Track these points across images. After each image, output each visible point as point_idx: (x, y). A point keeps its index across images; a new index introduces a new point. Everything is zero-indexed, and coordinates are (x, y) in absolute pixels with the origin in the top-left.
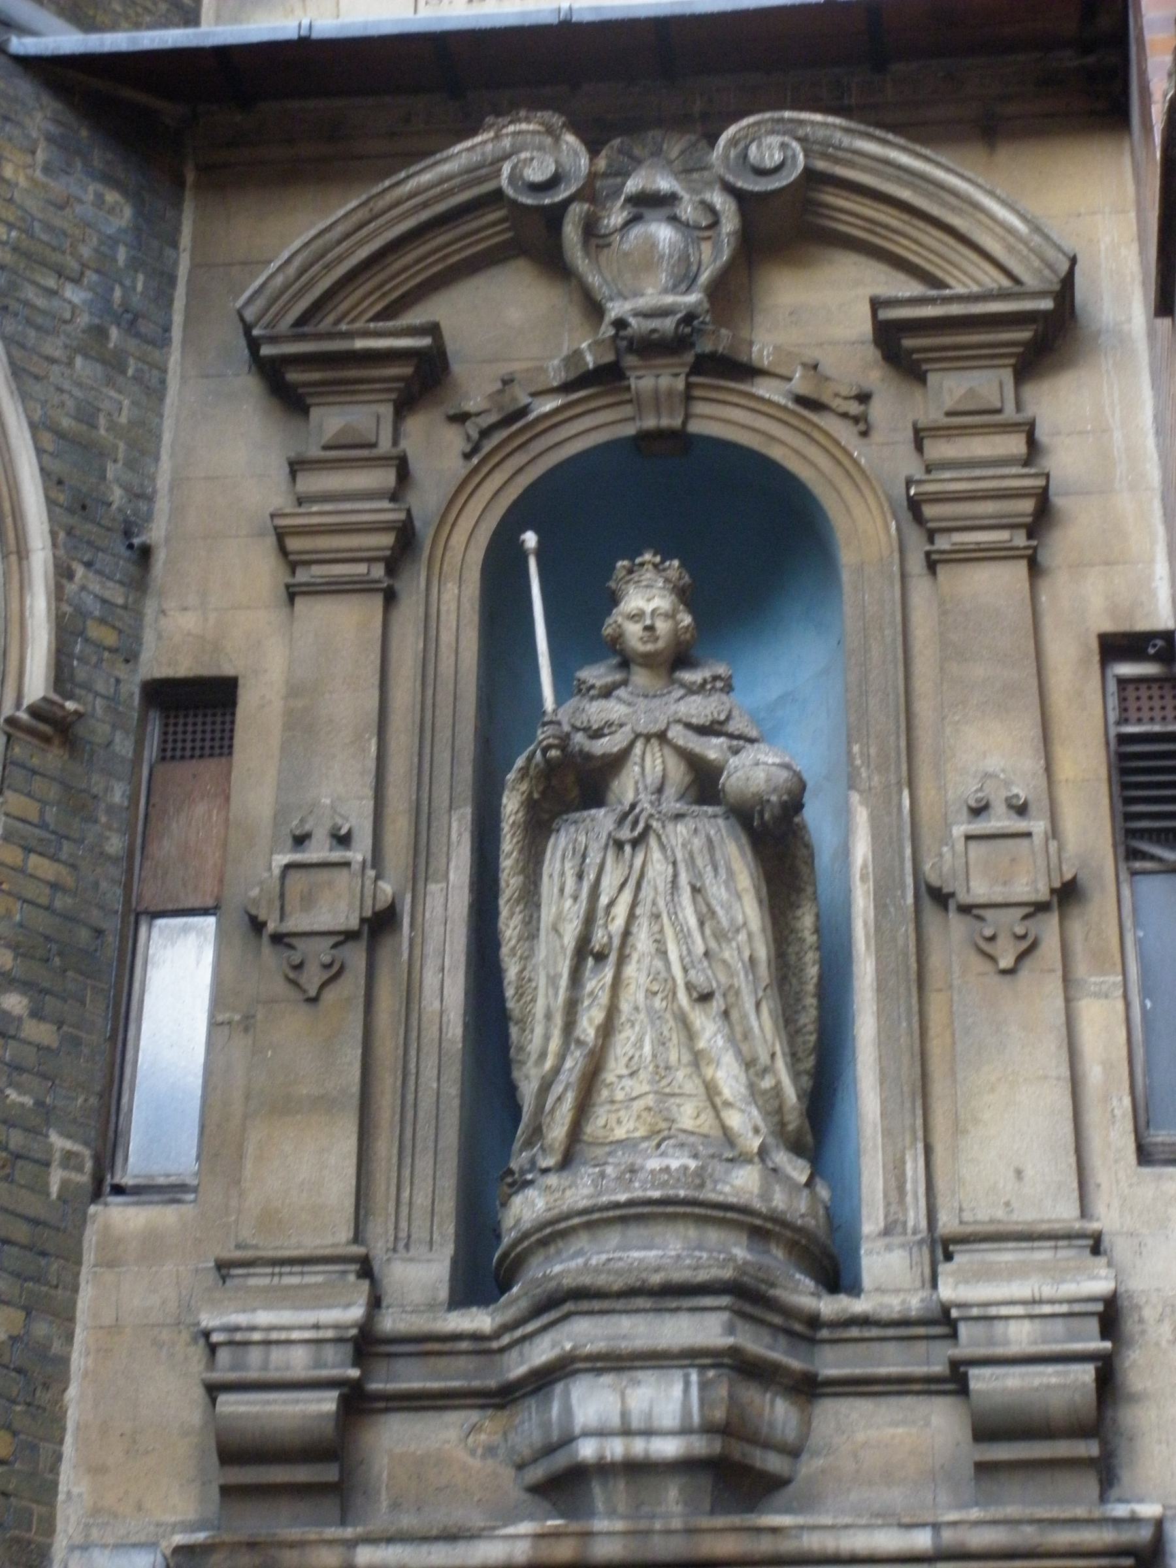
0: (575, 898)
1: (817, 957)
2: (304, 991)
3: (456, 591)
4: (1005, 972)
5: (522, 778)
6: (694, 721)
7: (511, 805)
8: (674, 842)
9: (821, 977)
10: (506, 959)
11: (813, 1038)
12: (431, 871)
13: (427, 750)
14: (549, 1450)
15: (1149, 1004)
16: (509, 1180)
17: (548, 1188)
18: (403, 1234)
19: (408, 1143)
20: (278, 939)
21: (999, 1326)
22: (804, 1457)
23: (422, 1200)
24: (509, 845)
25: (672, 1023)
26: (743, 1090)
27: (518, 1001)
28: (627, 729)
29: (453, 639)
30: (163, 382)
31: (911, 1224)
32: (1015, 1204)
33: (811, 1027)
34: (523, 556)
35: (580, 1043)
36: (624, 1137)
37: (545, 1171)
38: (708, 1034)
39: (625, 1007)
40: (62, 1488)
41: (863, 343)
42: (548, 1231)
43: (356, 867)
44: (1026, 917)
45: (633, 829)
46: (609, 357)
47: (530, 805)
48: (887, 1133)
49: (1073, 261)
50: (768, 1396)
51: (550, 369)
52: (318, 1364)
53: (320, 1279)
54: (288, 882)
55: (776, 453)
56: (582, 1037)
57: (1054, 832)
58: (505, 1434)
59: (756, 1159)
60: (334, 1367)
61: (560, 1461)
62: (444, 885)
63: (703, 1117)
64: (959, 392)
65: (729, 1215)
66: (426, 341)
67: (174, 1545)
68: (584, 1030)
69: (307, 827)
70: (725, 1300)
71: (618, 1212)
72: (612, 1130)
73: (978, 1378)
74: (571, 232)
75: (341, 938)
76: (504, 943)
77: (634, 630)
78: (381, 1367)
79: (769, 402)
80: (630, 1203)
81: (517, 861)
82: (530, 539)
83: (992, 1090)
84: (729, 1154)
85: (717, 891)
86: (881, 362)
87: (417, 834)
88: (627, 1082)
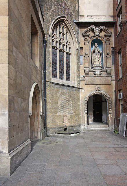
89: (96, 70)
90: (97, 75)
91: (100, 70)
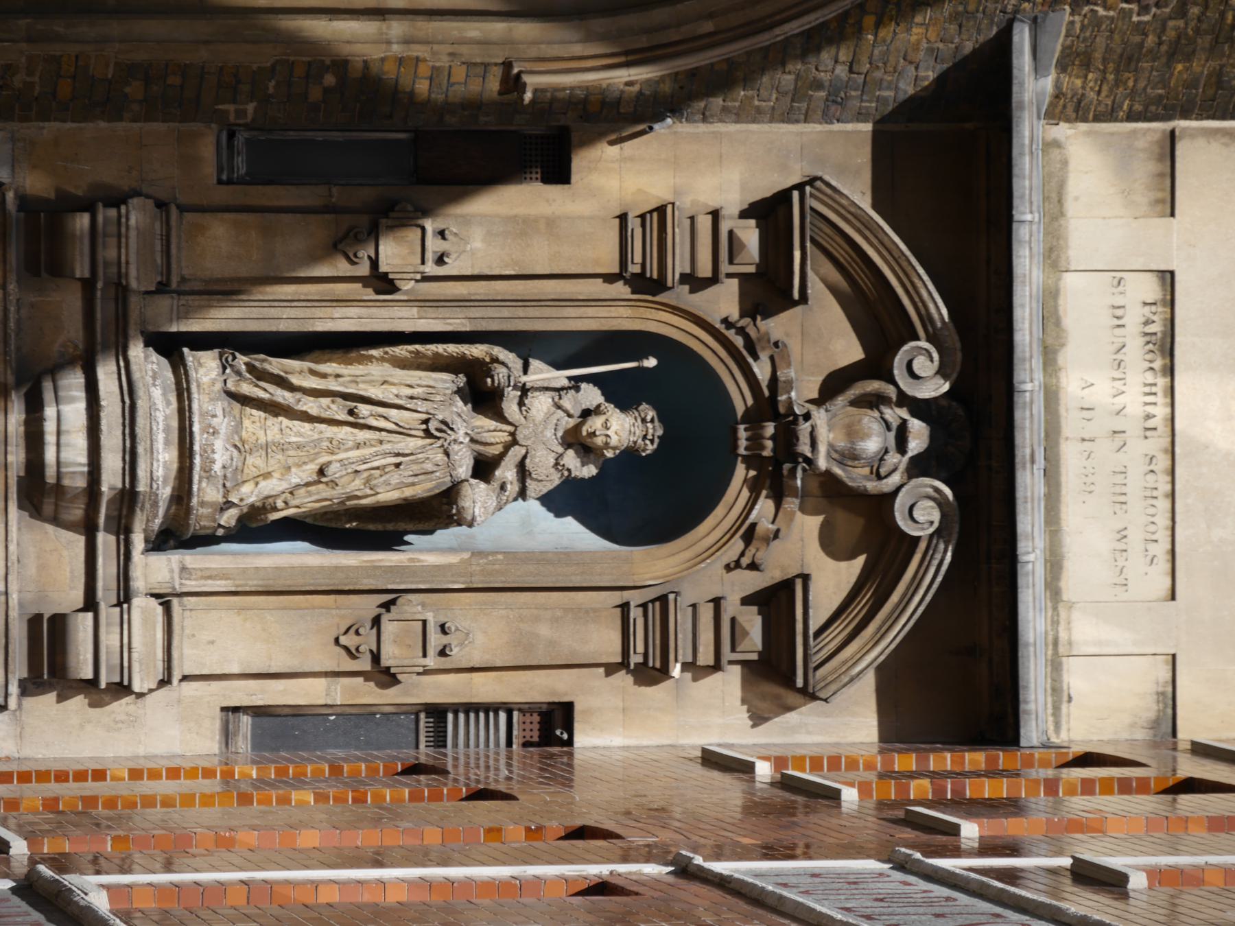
4: (337, 640)
6: (528, 461)
7: (477, 351)
15: (332, 718)
17: (214, 384)
24: (452, 349)
30: (797, 121)
34: (638, 358)
40: (46, 124)
46: (782, 410)
48: (244, 570)
49: (826, 700)
52: (106, 264)
53: (159, 261)
55: (719, 511)
57: (427, 672)
60: (105, 273)
64: (747, 626)
66: (796, 295)
74: (874, 386)
80: (191, 433)
82: (651, 362)
84: (228, 484)
91: (112, 478)
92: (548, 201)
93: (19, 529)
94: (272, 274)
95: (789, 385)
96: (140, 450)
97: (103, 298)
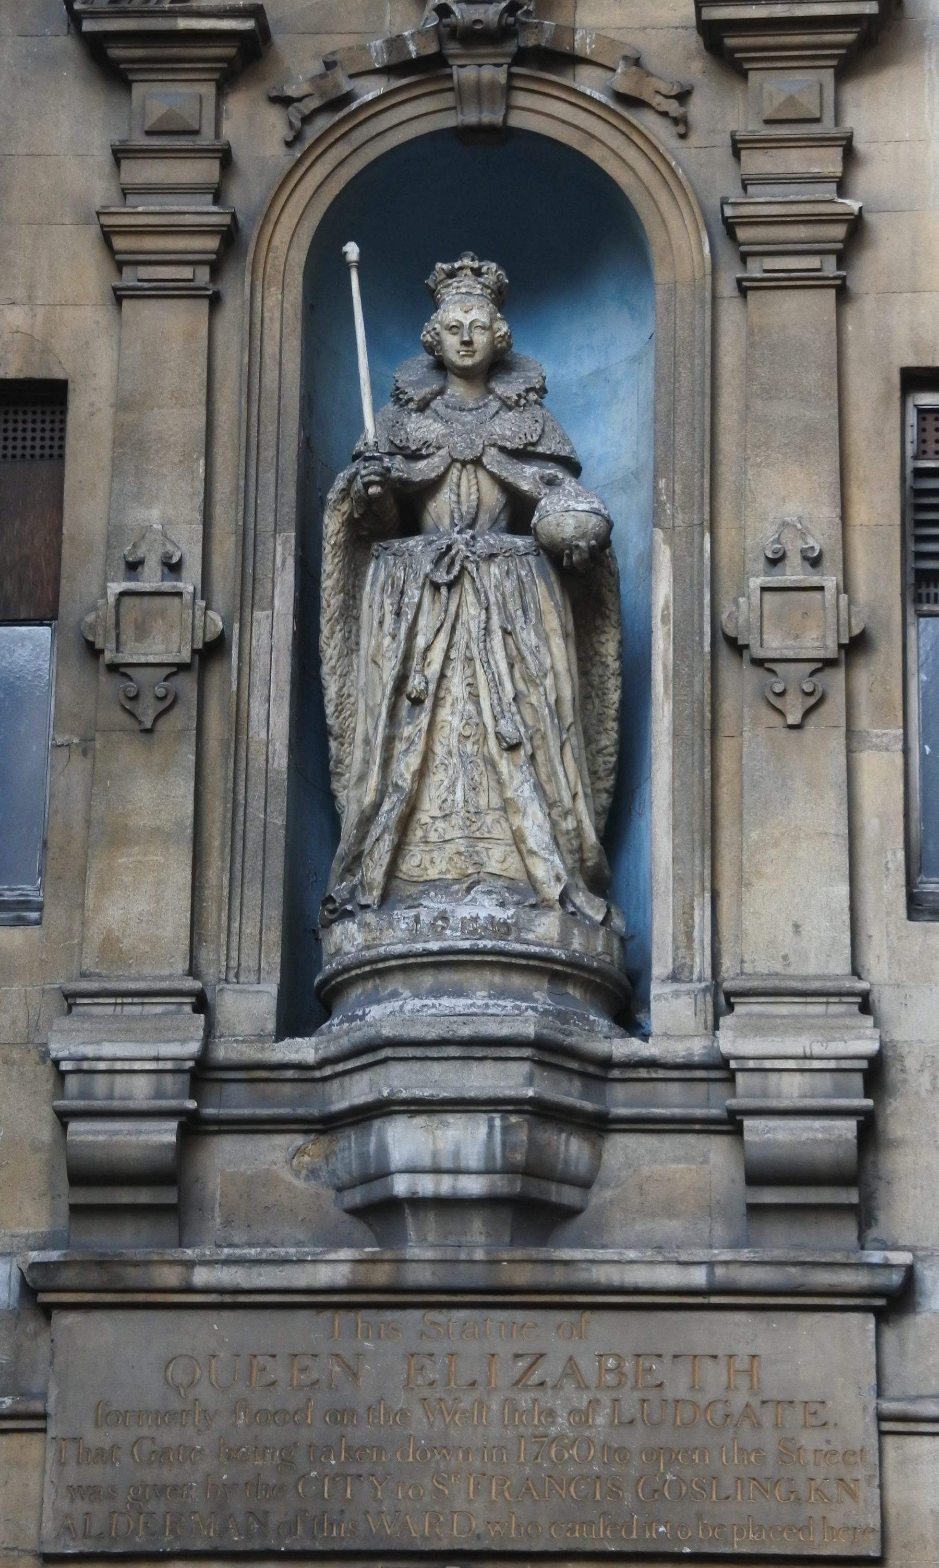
0: (394, 637)
1: (619, 683)
2: (140, 722)
3: (280, 297)
5: (343, 500)
6: (508, 445)
7: (332, 525)
8: (486, 583)
9: (623, 702)
10: (327, 677)
11: (614, 759)
12: (257, 597)
13: (253, 471)
14: (366, 1179)
15: (927, 749)
16: (330, 907)
18: (233, 964)
19: (238, 875)
20: (114, 668)
21: (774, 1077)
22: (595, 1188)
23: (250, 929)
25: (482, 768)
26: (547, 838)
27: (338, 717)
28: (443, 452)
29: (277, 350)
31: (696, 970)
32: (792, 958)
33: (611, 750)
34: (346, 267)
35: (397, 786)
36: (437, 877)
37: (365, 907)
38: (516, 782)
39: (439, 750)
41: (686, 28)
42: (367, 968)
43: (187, 597)
44: (812, 674)
45: (448, 573)
46: (432, 49)
47: (351, 524)
48: (677, 879)
50: (564, 1136)
51: (373, 49)
52: (159, 1094)
53: (159, 1009)
54: (122, 610)
55: (595, 153)
56: (400, 783)
57: (846, 587)
58: (327, 1158)
59: (558, 906)
61: (375, 1191)
62: (270, 612)
63: (510, 860)
64: (780, 99)
65: (531, 963)
67: (31, 1261)
68: (401, 775)
69: (140, 553)
70: (527, 1052)
71: (431, 959)
72: (426, 869)
73: (753, 1130)
75: (175, 669)
76: (325, 662)
77: (451, 342)
78: (213, 1090)
79: (590, 99)
81: (338, 580)
82: (352, 250)
83: (776, 844)
84: (533, 901)
85: (528, 637)
86: (705, 53)
87: (244, 559)
88: (440, 824)
89: (400, 1080)
90: (422, 1253)
92: (93, 414)
93: (604, 1247)
94: (189, 831)
95: (395, 43)
96: (466, 1031)
97: (219, 1107)
